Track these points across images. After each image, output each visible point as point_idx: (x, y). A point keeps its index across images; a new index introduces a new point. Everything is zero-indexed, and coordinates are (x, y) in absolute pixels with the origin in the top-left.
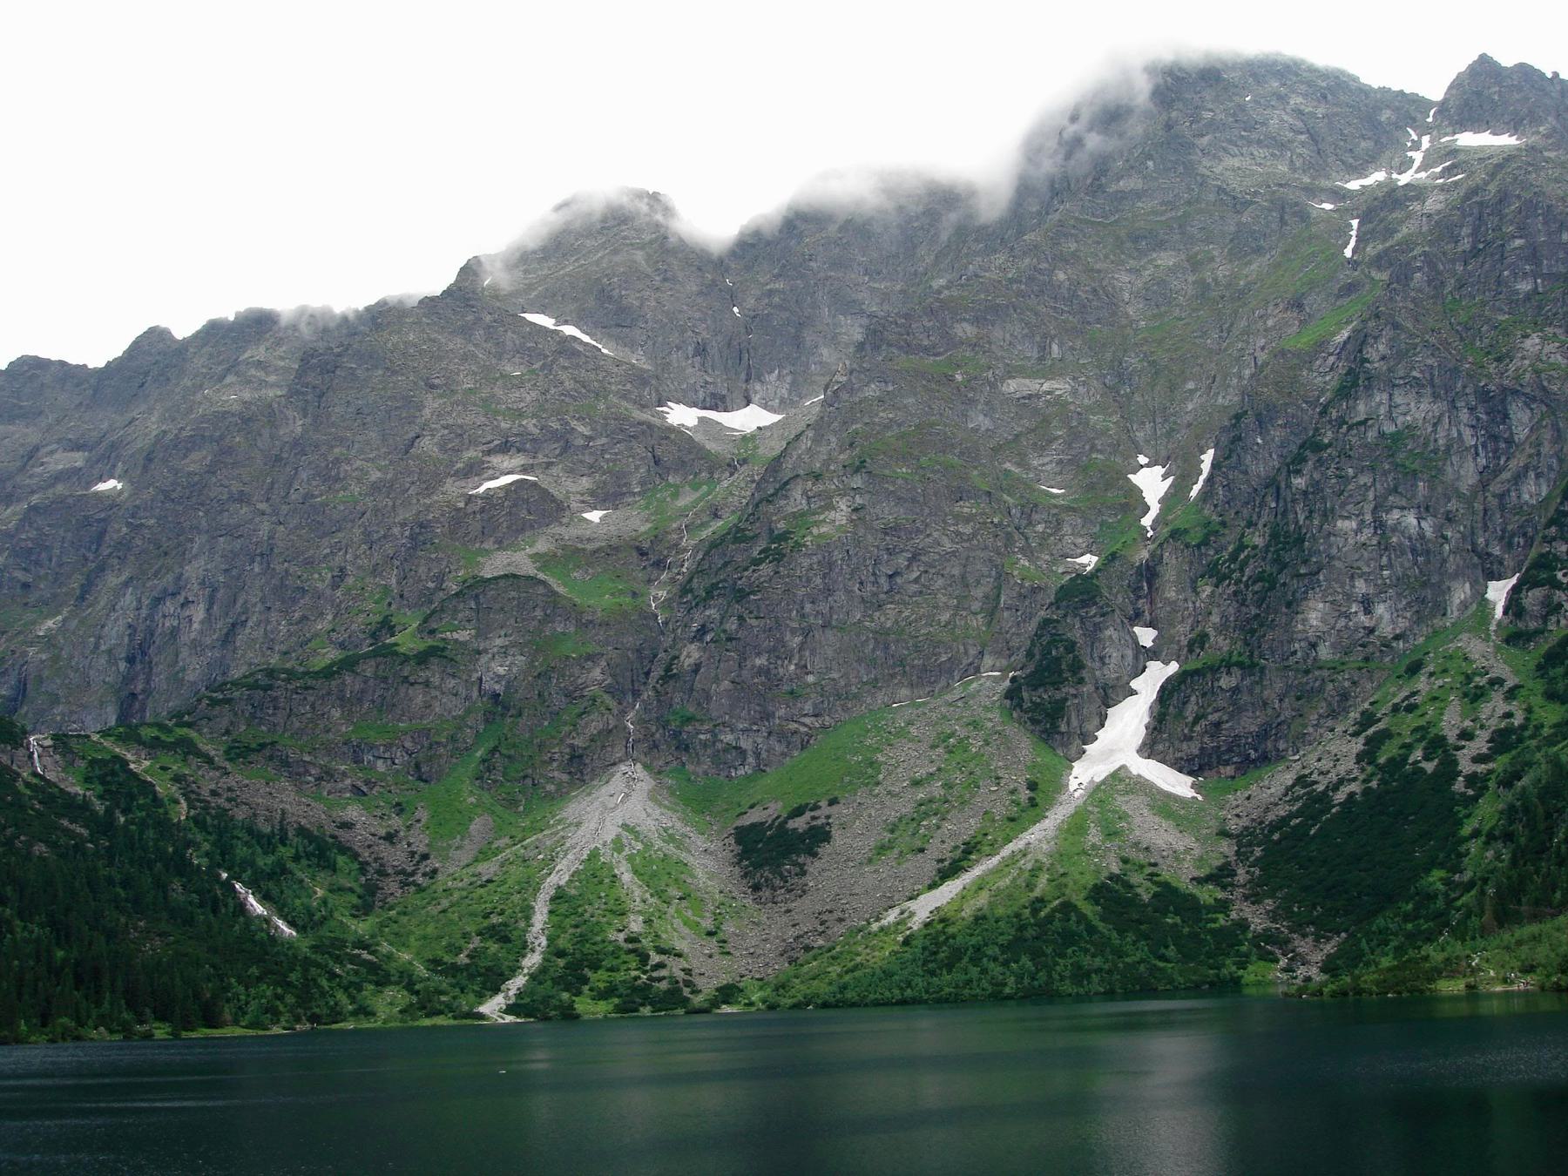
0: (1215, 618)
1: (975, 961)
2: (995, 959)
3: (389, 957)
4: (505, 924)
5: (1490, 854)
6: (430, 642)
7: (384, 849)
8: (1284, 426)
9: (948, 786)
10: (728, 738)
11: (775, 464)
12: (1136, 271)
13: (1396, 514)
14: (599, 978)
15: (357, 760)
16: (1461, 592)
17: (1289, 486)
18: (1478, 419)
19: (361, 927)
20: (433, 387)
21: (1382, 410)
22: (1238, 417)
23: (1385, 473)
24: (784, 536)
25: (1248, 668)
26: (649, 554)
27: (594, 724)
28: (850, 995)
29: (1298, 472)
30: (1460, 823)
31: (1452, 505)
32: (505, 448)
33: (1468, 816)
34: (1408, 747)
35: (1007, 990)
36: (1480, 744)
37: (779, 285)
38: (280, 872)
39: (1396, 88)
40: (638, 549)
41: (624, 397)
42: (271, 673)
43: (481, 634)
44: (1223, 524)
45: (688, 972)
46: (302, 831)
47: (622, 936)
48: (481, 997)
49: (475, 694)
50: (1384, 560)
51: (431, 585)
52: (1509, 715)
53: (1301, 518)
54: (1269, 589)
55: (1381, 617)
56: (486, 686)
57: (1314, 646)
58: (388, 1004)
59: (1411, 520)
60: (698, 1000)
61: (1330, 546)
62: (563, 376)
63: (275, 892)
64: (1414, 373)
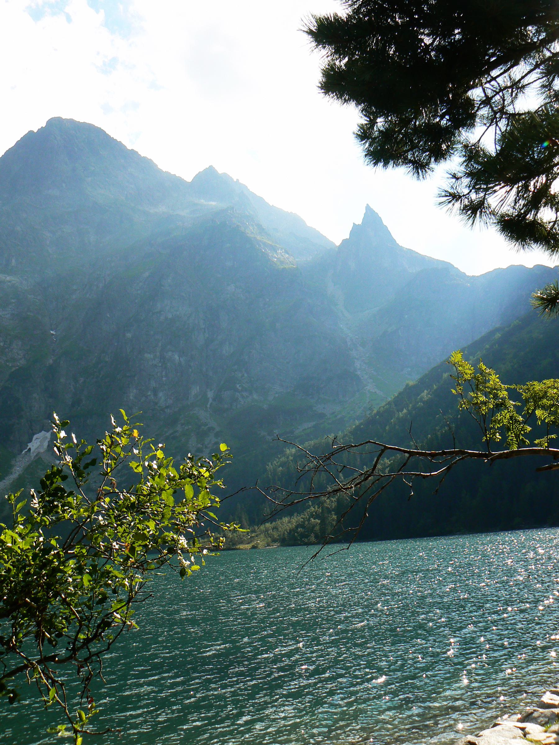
13: (170, 354)
39: (172, 173)
50: (164, 373)
59: (177, 357)
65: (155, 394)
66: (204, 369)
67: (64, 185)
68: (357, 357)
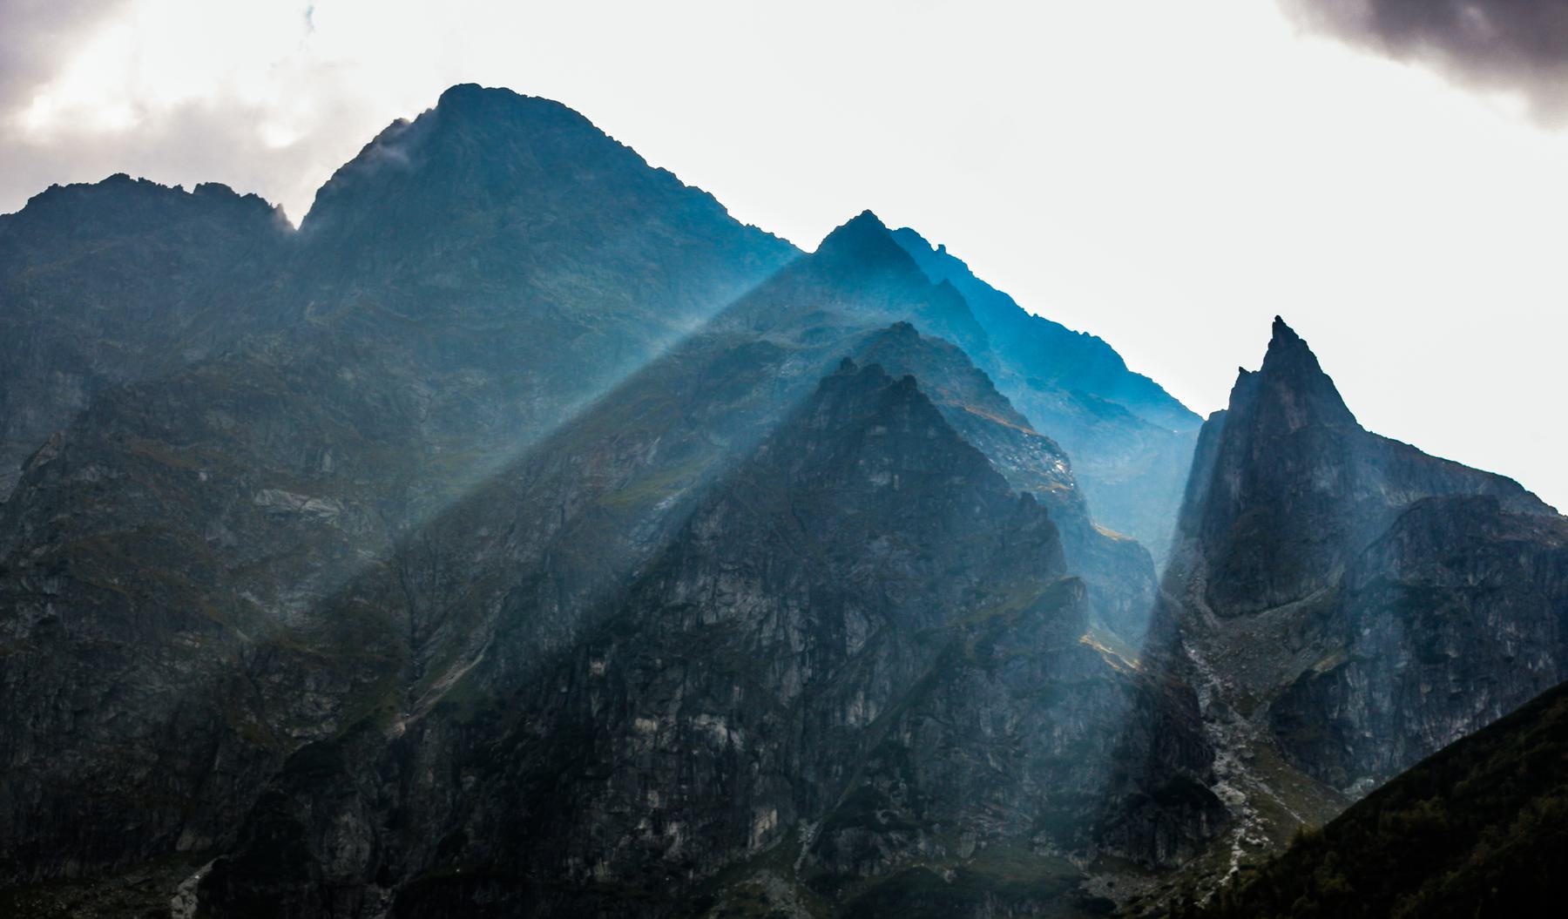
0: (477, 817)
13: (704, 720)
16: (766, 821)
17: (587, 668)
18: (809, 622)
21: (703, 598)
29: (599, 656)
53: (595, 709)
55: (672, 839)
57: (591, 863)
59: (722, 729)
61: (625, 745)
65: (658, 829)
66: (796, 762)
68: (1223, 742)
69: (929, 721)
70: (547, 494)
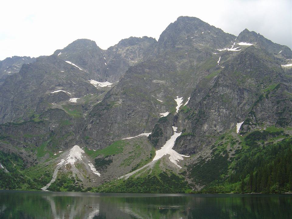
1: (136, 186)
2: (140, 186)
3: (26, 178)
4: (49, 173)
5: (233, 172)
6: (41, 120)
7: (28, 158)
8: (203, 92)
9: (136, 154)
10: (95, 142)
11: (109, 92)
12: (180, 63)
13: (222, 110)
14: (65, 185)
15: (25, 141)
16: (232, 125)
19: (22, 172)
20: (47, 73)
22: (195, 90)
23: (220, 102)
24: (109, 105)
25: (193, 136)
26: (84, 107)
27: (70, 138)
28: (112, 191)
30: (228, 166)
31: (232, 109)
32: (59, 85)
33: (230, 165)
34: (220, 152)
35: (141, 191)
36: (233, 152)
37: (114, 59)
38: (7, 161)
40: (82, 106)
41: (83, 77)
42: (10, 123)
43: (51, 119)
44: (191, 109)
45: (82, 184)
46: (13, 153)
47: (71, 177)
48: (42, 187)
49: (48, 130)
50: (219, 118)
51: (42, 109)
52: (239, 147)
54: (198, 121)
56: (50, 129)
58: (25, 186)
59: (225, 111)
60: (83, 190)
62: (71, 73)
63: (6, 164)
64: (227, 84)
66: (237, 116)
67: (184, 43)
69: (258, 107)
70: (197, 77)
